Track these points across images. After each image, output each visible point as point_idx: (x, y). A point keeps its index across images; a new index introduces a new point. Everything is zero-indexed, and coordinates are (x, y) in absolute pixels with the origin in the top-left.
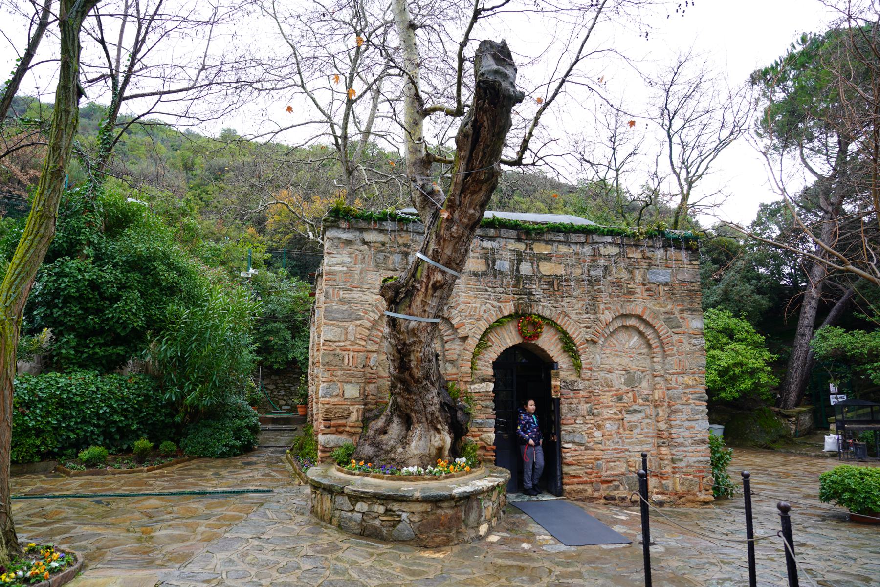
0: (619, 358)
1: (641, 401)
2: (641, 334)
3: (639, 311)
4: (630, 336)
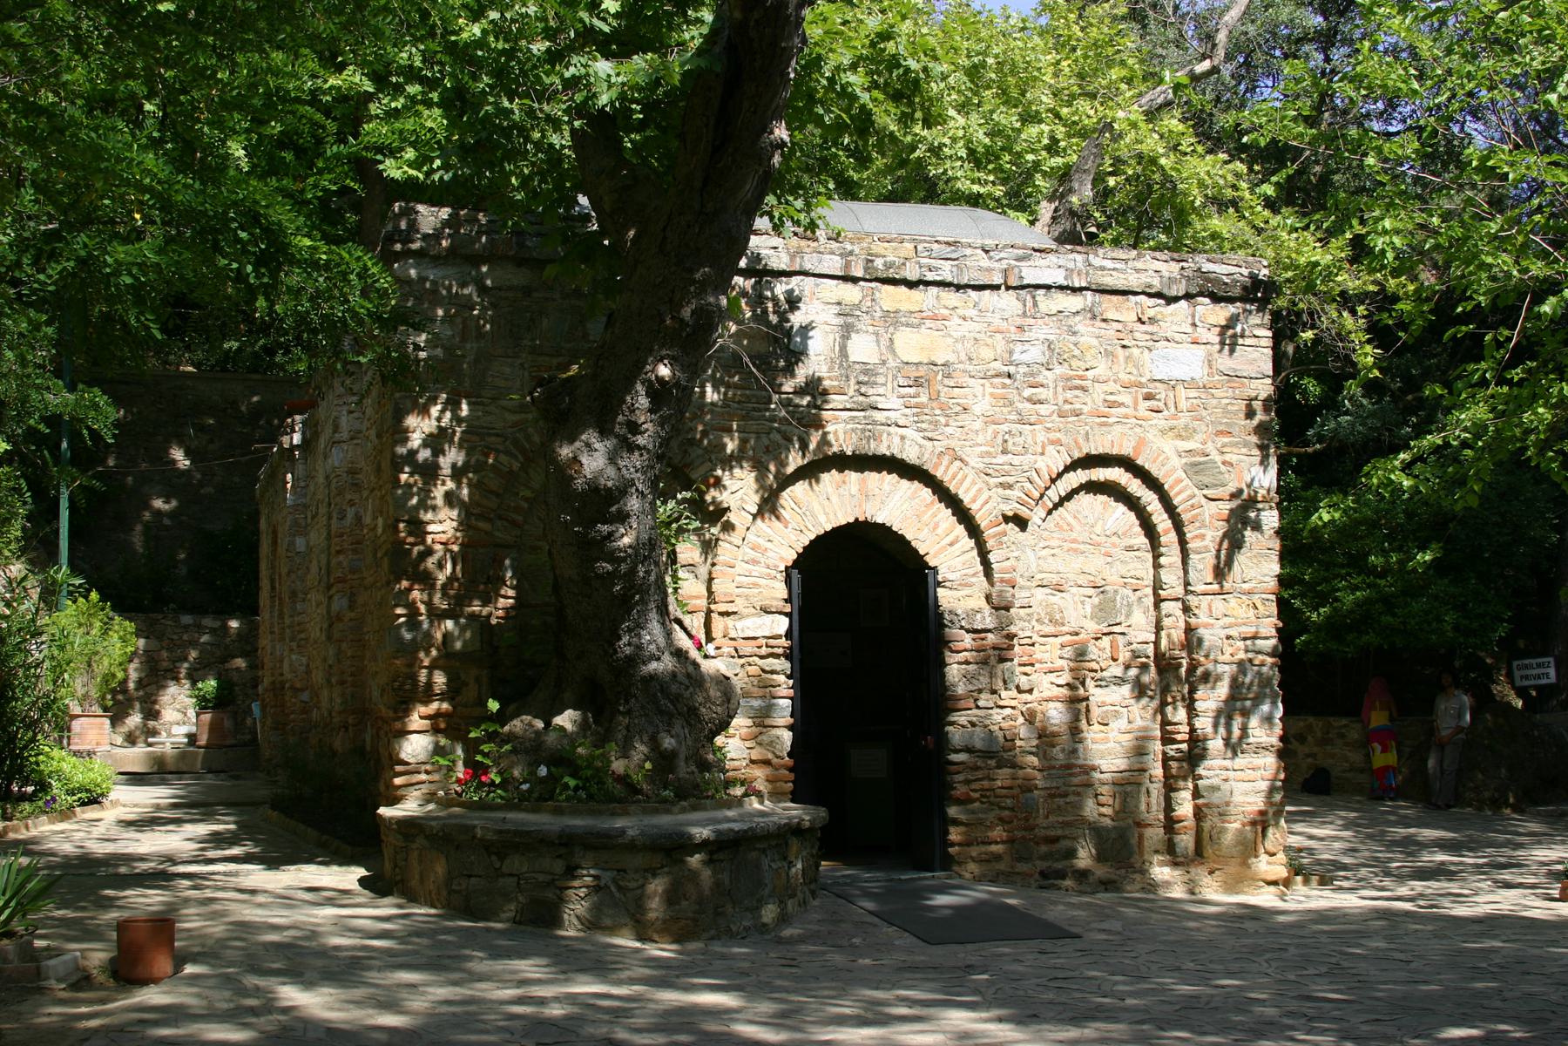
0: (1081, 558)
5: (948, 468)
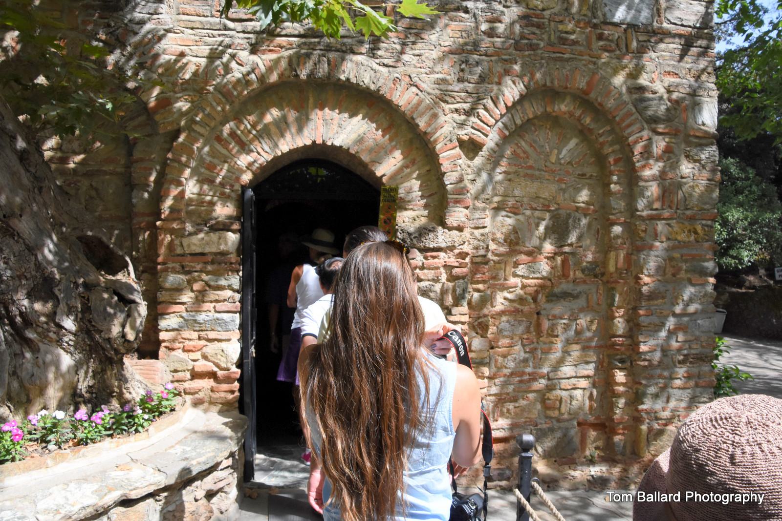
0: (536, 184)
1: (579, 274)
2: (584, 134)
3: (581, 83)
4: (564, 140)
5: (403, 93)
